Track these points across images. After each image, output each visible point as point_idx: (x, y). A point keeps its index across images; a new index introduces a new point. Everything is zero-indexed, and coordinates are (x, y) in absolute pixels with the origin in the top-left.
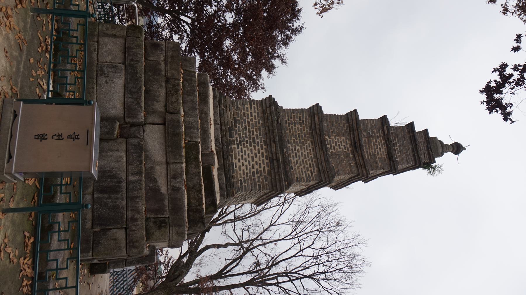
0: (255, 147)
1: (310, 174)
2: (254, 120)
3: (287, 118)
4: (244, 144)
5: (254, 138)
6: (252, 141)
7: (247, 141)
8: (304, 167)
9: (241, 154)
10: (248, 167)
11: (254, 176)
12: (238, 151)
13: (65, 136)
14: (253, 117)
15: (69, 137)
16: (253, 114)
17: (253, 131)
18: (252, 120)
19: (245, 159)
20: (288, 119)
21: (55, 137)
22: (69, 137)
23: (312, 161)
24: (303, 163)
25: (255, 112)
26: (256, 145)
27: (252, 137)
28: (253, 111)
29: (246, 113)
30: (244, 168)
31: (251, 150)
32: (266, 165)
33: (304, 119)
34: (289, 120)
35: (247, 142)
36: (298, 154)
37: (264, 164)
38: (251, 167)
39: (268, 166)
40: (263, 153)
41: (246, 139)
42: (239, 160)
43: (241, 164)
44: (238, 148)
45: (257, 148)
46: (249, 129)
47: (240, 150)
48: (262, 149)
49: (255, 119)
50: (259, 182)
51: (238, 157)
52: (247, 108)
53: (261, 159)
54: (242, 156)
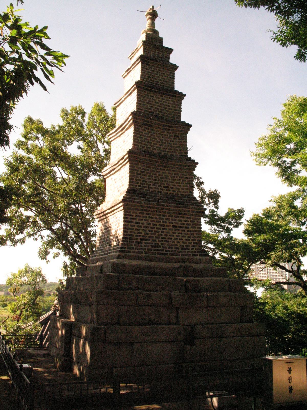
0: (167, 226)
1: (188, 179)
2: (143, 222)
3: (138, 187)
4: (165, 235)
5: (160, 225)
6: (162, 227)
7: (162, 232)
8: (182, 183)
9: (173, 240)
10: (183, 235)
11: (191, 231)
12: (171, 242)
13: (289, 376)
14: (141, 222)
15: (290, 373)
16: (137, 221)
17: (154, 225)
18: (143, 223)
19: (177, 236)
20: (140, 186)
21: (290, 382)
22: (290, 373)
23: (178, 174)
24: (179, 183)
25: (135, 219)
26: (165, 224)
27: (158, 226)
28: (135, 221)
29: (136, 227)
30: (184, 239)
31: (169, 229)
32: (183, 219)
33: (140, 170)
34: (140, 186)
35: (163, 232)
36: (171, 186)
37: (181, 221)
38: (183, 232)
39: (184, 217)
40: (172, 220)
41: (160, 233)
42: (178, 242)
43: (181, 242)
44: (168, 242)
45: (168, 224)
46: (151, 227)
47: (170, 240)
48: (168, 219)
49: (142, 220)
50: (195, 228)
51: (176, 243)
52: (131, 226)
53: (177, 222)
54: (175, 239)
